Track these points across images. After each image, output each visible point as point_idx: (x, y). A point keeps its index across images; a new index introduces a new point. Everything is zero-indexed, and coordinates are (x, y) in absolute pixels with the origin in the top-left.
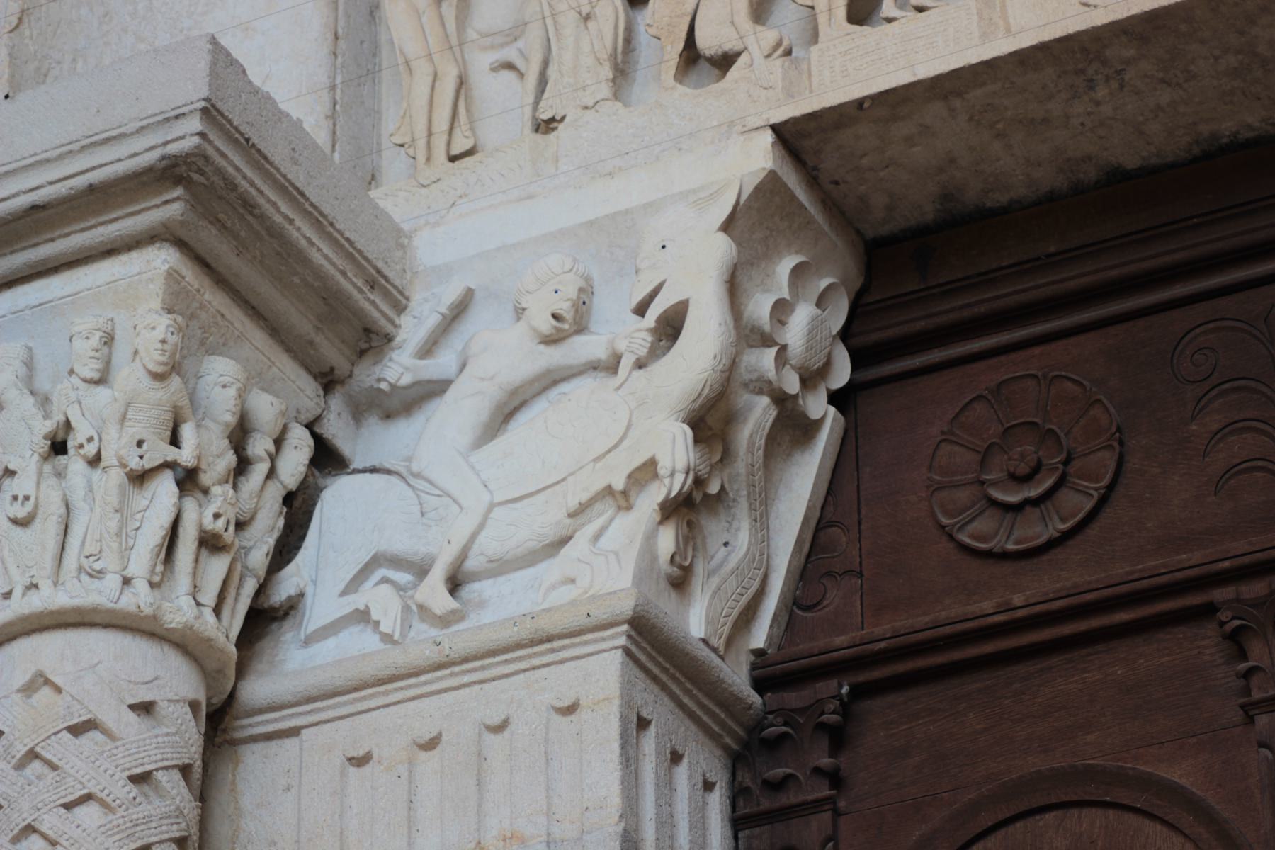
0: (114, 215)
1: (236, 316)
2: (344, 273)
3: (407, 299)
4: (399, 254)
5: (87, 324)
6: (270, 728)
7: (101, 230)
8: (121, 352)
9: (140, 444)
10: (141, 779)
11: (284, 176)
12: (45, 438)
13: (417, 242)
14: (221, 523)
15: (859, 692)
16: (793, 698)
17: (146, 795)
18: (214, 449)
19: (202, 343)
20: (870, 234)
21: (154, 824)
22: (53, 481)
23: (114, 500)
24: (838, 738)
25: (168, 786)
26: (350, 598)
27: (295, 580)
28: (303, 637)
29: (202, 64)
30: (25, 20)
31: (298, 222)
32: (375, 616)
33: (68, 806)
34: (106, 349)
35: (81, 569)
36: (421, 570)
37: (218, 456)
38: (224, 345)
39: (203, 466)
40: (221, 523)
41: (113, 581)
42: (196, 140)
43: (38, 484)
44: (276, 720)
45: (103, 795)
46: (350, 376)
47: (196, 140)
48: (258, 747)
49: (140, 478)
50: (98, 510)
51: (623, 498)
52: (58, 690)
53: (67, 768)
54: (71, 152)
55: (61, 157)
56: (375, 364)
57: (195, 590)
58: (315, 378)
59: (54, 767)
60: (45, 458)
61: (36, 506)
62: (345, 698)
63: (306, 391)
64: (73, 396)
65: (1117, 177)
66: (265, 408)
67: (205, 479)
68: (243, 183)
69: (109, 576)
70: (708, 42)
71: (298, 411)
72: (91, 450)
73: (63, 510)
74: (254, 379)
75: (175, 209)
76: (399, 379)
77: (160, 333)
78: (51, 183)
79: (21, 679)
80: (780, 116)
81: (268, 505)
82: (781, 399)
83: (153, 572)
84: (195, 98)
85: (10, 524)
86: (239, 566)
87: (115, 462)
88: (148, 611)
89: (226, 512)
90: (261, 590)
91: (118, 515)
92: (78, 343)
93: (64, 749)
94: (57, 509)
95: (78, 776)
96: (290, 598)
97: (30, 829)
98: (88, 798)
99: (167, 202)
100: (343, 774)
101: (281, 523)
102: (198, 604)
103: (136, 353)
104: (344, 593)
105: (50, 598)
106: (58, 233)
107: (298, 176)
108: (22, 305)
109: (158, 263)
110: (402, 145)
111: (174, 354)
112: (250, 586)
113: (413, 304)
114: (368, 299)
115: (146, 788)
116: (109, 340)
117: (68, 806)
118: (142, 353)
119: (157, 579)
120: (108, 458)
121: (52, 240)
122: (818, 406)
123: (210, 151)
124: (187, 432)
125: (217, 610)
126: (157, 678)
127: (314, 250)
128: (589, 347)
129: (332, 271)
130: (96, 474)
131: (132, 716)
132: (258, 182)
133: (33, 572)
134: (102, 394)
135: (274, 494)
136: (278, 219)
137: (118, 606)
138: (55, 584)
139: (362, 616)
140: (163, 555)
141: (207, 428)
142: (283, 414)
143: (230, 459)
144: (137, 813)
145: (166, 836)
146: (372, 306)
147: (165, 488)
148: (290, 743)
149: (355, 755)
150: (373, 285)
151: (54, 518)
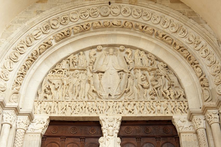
5: (24, 118)
15: (47, 137)
16: (45, 137)
20: (51, 120)
24: (46, 138)
36: (33, 129)
51: (41, 129)
65: (60, 121)
70: (47, 112)
80: (50, 116)
82: (47, 126)
93: (21, 134)
122: (48, 126)
128: (40, 122)
147: (26, 125)
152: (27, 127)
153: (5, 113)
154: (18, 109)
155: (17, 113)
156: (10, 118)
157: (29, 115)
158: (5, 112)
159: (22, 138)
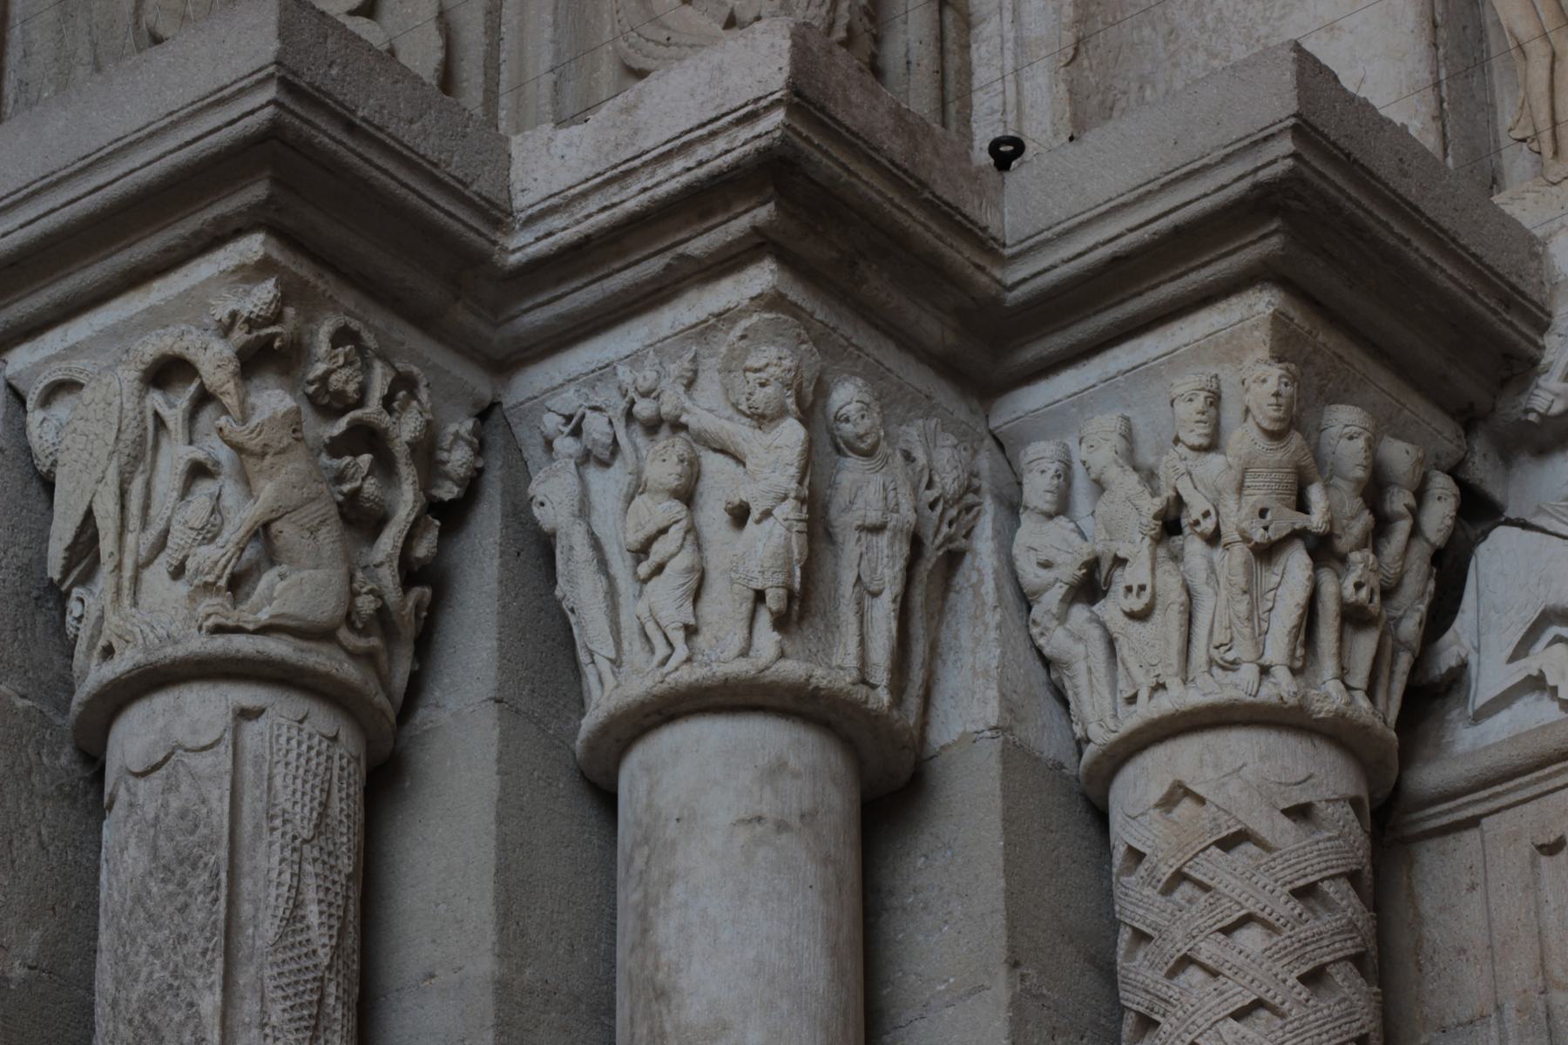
0: (1206, 258)
1: (1358, 360)
2: (1473, 294)
3: (1550, 315)
4: (1534, 264)
5: (1189, 383)
6: (1445, 820)
7: (1193, 276)
8: (1231, 412)
9: (1263, 513)
10: (1305, 893)
11: (1394, 192)
12: (1156, 517)
13: (1553, 248)
14: (1364, 593)
17: (1313, 911)
18: (1347, 510)
19: (1321, 391)
21: (1325, 942)
22: (1169, 566)
23: (1240, 580)
25: (1337, 897)
26: (1522, 663)
27: (1455, 649)
28: (1470, 712)
29: (1287, 76)
30: (1083, 49)
31: (1416, 243)
32: (1551, 681)
33: (1227, 931)
34: (1212, 411)
35: (1211, 662)
37: (1353, 518)
38: (1346, 391)
39: (1337, 532)
40: (1364, 593)
41: (1249, 673)
42: (1290, 162)
43: (1153, 570)
44: (1450, 811)
45: (1264, 915)
46: (1493, 410)
47: (1290, 162)
48: (1433, 844)
49: (1266, 553)
50: (1223, 593)
52: (1201, 800)
53: (1221, 887)
54: (1150, 192)
55: (1140, 199)
56: (1519, 394)
57: (1343, 674)
58: (1453, 416)
59: (1206, 888)
60: (1158, 541)
61: (1154, 596)
62: (1527, 778)
63: (1444, 434)
64: (1182, 467)
66: (1400, 455)
67: (1342, 544)
68: (1348, 204)
69: (1244, 667)
71: (1438, 457)
72: (1208, 525)
73: (1184, 598)
74: (1383, 426)
75: (1274, 242)
76: (1550, 407)
77: (1272, 385)
78: (1131, 230)
79: (1157, 792)
81: (1415, 567)
83: (1293, 656)
84: (1283, 116)
85: (1126, 619)
86: (1390, 641)
87: (1237, 537)
88: (1292, 701)
89: (1368, 581)
90: (1418, 665)
91: (1247, 597)
92: (1180, 407)
93: (1218, 868)
94: (1176, 596)
95: (1234, 895)
96: (1451, 670)
97: (1186, 961)
98: (1247, 920)
99: (1264, 237)
100: (1534, 864)
101: (1431, 586)
102: (1349, 688)
103: (1247, 411)
104: (1513, 658)
105: (1179, 698)
106: (1145, 285)
107: (1413, 193)
108: (1112, 372)
109: (1261, 306)
110: (1523, 140)
111: (1289, 408)
112: (1404, 662)
113: (1556, 320)
114: (1504, 321)
115: (1312, 902)
116: (1215, 399)
117: (1227, 931)
118: (1254, 410)
119: (1298, 664)
120: (1230, 533)
121: (1140, 294)
123: (1307, 172)
124: (1316, 494)
125: (1371, 693)
126: (1310, 777)
127: (1437, 272)
129: (1461, 294)
130: (1218, 554)
131: (1287, 823)
132: (1365, 201)
133: (1159, 670)
134: (1214, 461)
135: (1420, 553)
136: (1392, 241)
137: (1259, 699)
138: (1185, 681)
139: (1536, 683)
140: (1302, 637)
141: (1336, 487)
142: (1420, 461)
143: (1366, 518)
144: (1304, 931)
145: (1341, 954)
146: (1511, 326)
147: (1297, 564)
148: (1470, 837)
149: (1546, 841)
150: (1508, 303)
151: (1176, 607)
152: (1354, 618)
153: (566, 445)
154: (870, 185)
155: (934, 329)
156: (740, 515)
157: (1266, 244)
158: (570, 400)
159: (1287, 991)
